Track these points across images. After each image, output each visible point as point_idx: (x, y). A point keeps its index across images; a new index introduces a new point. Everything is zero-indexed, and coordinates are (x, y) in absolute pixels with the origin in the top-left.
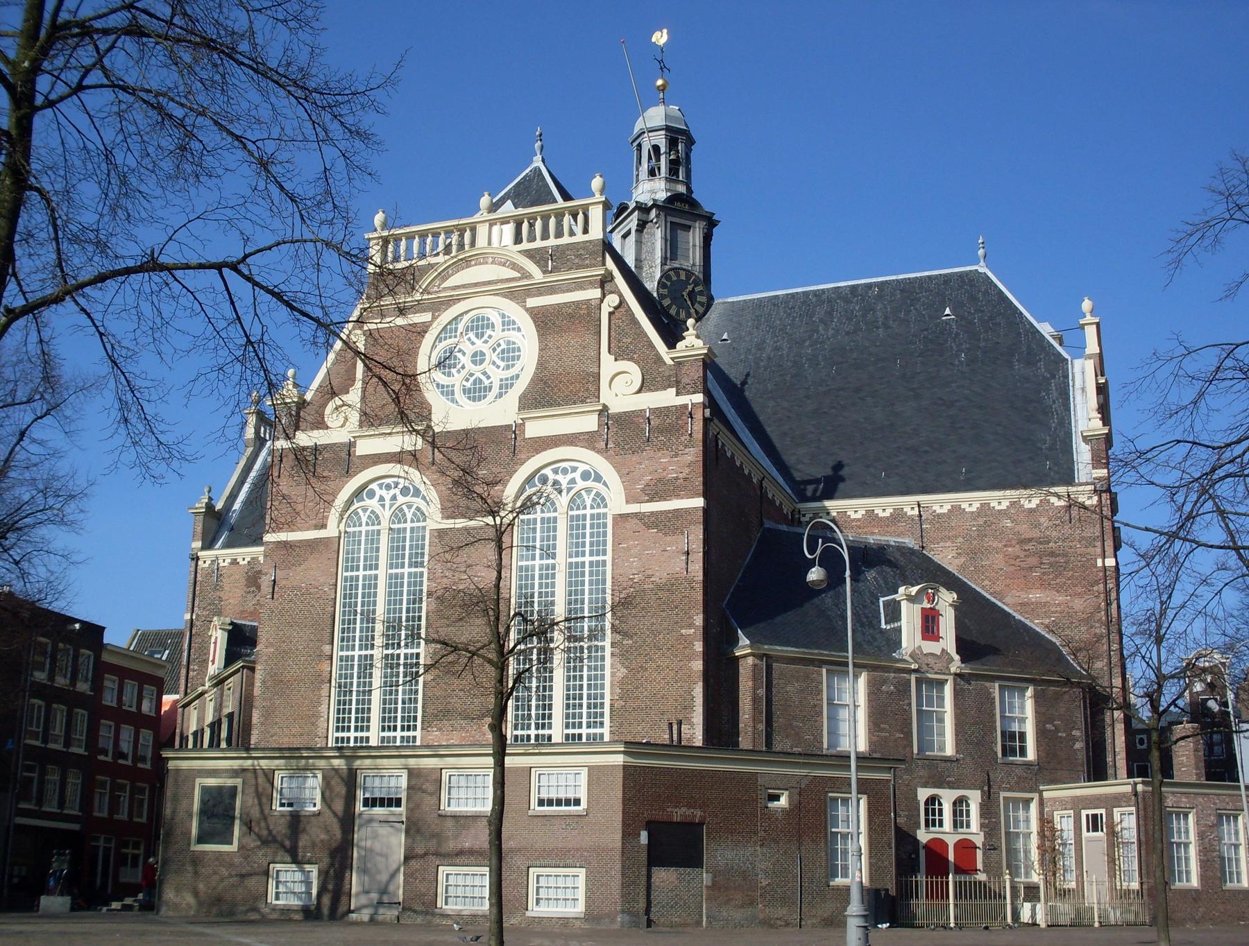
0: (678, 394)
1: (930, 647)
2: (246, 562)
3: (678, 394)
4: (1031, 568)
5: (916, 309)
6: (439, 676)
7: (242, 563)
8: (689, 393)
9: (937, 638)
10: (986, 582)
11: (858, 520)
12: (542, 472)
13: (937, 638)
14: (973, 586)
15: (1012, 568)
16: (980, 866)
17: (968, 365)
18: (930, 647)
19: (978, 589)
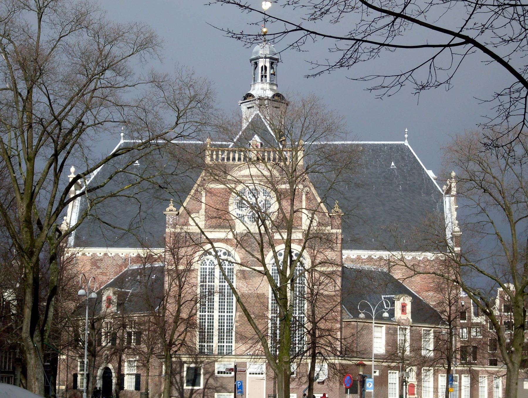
0: (332, 229)
1: (404, 317)
2: (90, 255)
3: (332, 229)
4: (430, 283)
5: (379, 161)
6: (241, 324)
7: (88, 255)
8: (336, 228)
9: (405, 313)
10: (413, 287)
11: (364, 259)
12: (280, 252)
13: (405, 313)
14: (408, 288)
15: (423, 283)
16: (416, 393)
17: (403, 192)
18: (404, 317)
19: (411, 290)
